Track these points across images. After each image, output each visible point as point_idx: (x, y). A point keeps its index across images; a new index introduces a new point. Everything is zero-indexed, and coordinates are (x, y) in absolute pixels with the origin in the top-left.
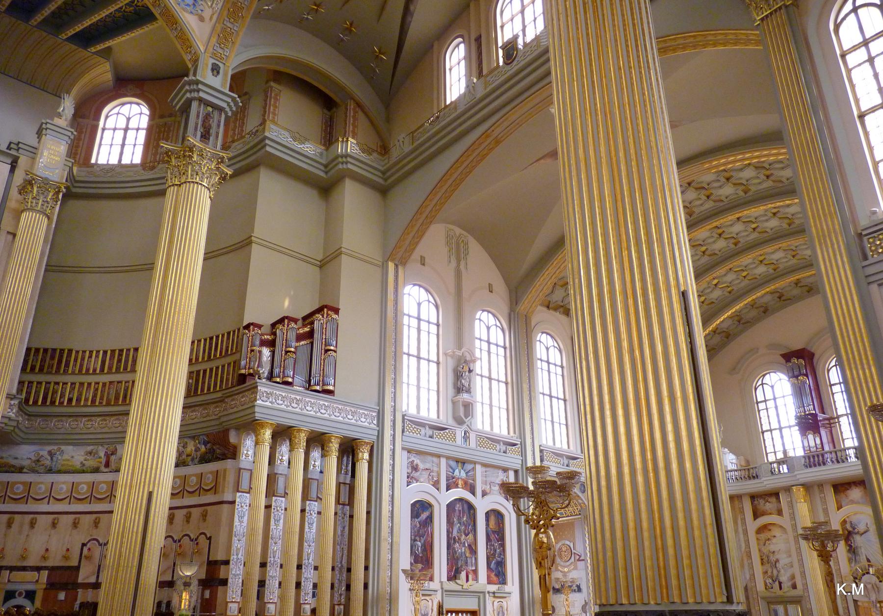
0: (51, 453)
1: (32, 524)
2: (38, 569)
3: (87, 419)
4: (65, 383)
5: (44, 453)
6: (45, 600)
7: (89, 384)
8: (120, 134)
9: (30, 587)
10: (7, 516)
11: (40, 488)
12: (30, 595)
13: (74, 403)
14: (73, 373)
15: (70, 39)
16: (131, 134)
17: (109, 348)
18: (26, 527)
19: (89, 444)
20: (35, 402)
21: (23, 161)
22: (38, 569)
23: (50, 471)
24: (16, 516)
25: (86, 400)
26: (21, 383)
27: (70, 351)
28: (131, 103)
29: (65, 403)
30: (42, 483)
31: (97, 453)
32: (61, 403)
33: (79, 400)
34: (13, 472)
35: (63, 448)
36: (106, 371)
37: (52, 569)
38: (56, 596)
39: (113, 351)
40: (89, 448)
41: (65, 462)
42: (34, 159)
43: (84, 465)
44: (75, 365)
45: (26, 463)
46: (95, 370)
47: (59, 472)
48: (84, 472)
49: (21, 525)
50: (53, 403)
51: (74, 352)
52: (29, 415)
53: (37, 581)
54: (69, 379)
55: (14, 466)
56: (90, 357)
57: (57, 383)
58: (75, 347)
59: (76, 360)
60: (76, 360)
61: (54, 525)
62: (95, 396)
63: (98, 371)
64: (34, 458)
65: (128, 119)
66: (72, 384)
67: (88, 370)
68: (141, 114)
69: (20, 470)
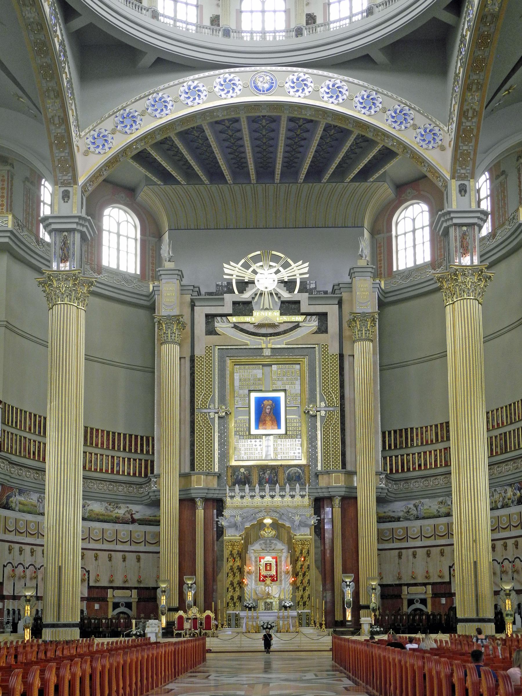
0: (416, 506)
1: (414, 555)
2: (425, 584)
3: (434, 478)
4: (413, 454)
5: (411, 506)
6: (433, 604)
7: (430, 452)
9: (423, 597)
10: (397, 551)
11: (414, 531)
12: (424, 602)
13: (423, 468)
14: (417, 445)
17: (438, 422)
18: (411, 557)
19: (439, 497)
20: (397, 471)
21: (345, 296)
22: (425, 584)
23: (417, 518)
24: (402, 550)
25: (431, 464)
26: (385, 458)
27: (412, 429)
29: (417, 469)
30: (414, 527)
31: (446, 502)
32: (414, 469)
33: (425, 465)
34: (394, 521)
35: (422, 501)
36: (440, 441)
37: (433, 584)
38: (440, 601)
39: (442, 424)
40: (440, 499)
41: (427, 511)
42: (351, 292)
43: (439, 512)
44: (417, 439)
45: (401, 514)
46: (432, 441)
47: (424, 518)
48: (439, 517)
49: (408, 556)
50: (408, 470)
51: (415, 430)
52: (395, 481)
53: (426, 592)
54: (416, 450)
55: (394, 517)
56: (427, 431)
57: (408, 455)
58: (415, 425)
59: (417, 435)
60: (417, 435)
61: (428, 555)
62: (436, 461)
63: (434, 442)
64: (405, 510)
66: (418, 454)
67: (427, 442)
69: (398, 519)
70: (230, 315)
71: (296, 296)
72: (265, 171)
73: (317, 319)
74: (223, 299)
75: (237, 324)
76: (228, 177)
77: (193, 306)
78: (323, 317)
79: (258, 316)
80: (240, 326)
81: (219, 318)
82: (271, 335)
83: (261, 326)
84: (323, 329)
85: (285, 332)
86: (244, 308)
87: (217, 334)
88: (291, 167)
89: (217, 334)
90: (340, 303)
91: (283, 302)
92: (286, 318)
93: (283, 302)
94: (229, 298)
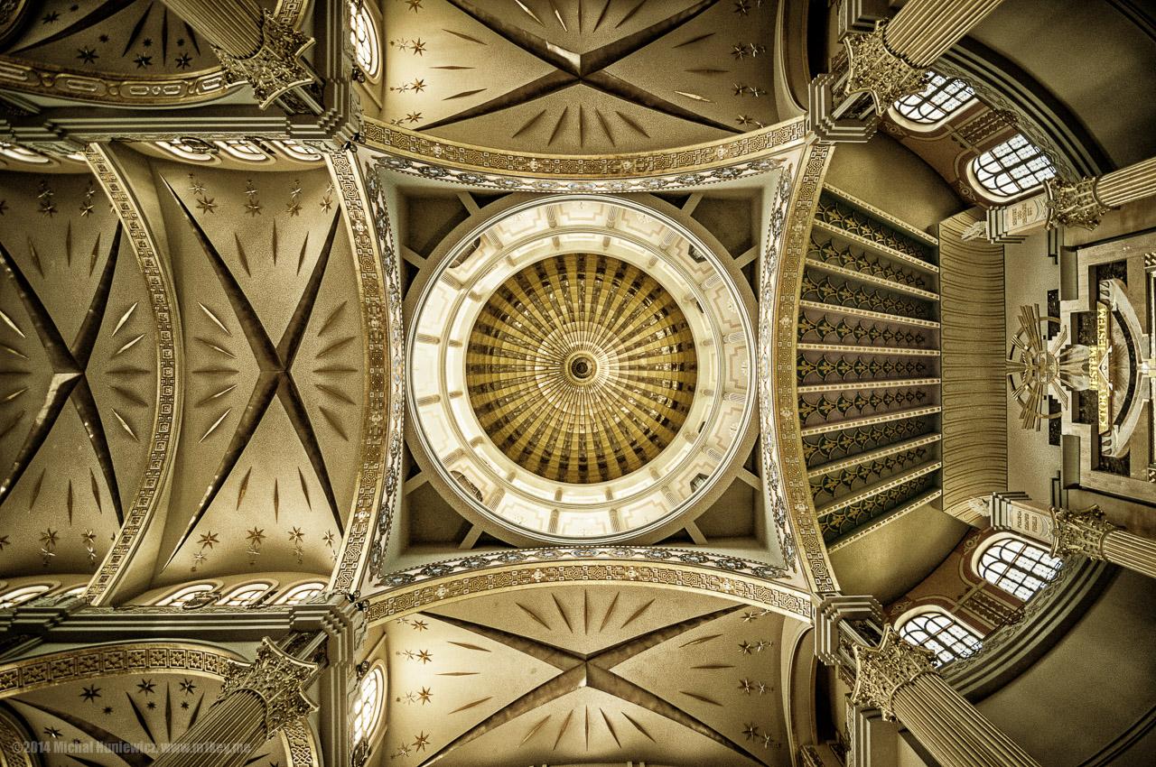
8: (1016, 173)
15: (935, 263)
16: (1007, 162)
28: (980, 183)
65: (996, 175)
68: (982, 167)
70: (1095, 429)
71: (1065, 320)
72: (926, 368)
73: (1104, 282)
74: (1067, 437)
75: (1114, 419)
76: (936, 410)
77: (1076, 486)
78: (1099, 273)
79: (1098, 381)
80: (1116, 414)
81: (1105, 448)
82: (1133, 360)
83: (1115, 377)
84: (1116, 270)
85: (1127, 335)
86: (1085, 406)
87: (1127, 457)
88: (920, 338)
89: (1127, 457)
90: (1075, 249)
91: (1077, 340)
92: (1102, 336)
93: (1077, 340)
94: (1068, 428)
